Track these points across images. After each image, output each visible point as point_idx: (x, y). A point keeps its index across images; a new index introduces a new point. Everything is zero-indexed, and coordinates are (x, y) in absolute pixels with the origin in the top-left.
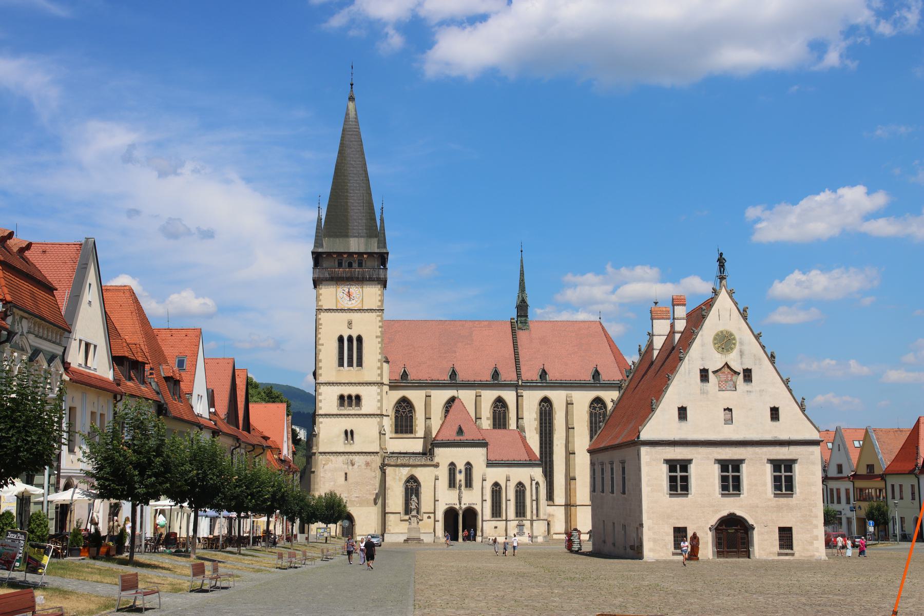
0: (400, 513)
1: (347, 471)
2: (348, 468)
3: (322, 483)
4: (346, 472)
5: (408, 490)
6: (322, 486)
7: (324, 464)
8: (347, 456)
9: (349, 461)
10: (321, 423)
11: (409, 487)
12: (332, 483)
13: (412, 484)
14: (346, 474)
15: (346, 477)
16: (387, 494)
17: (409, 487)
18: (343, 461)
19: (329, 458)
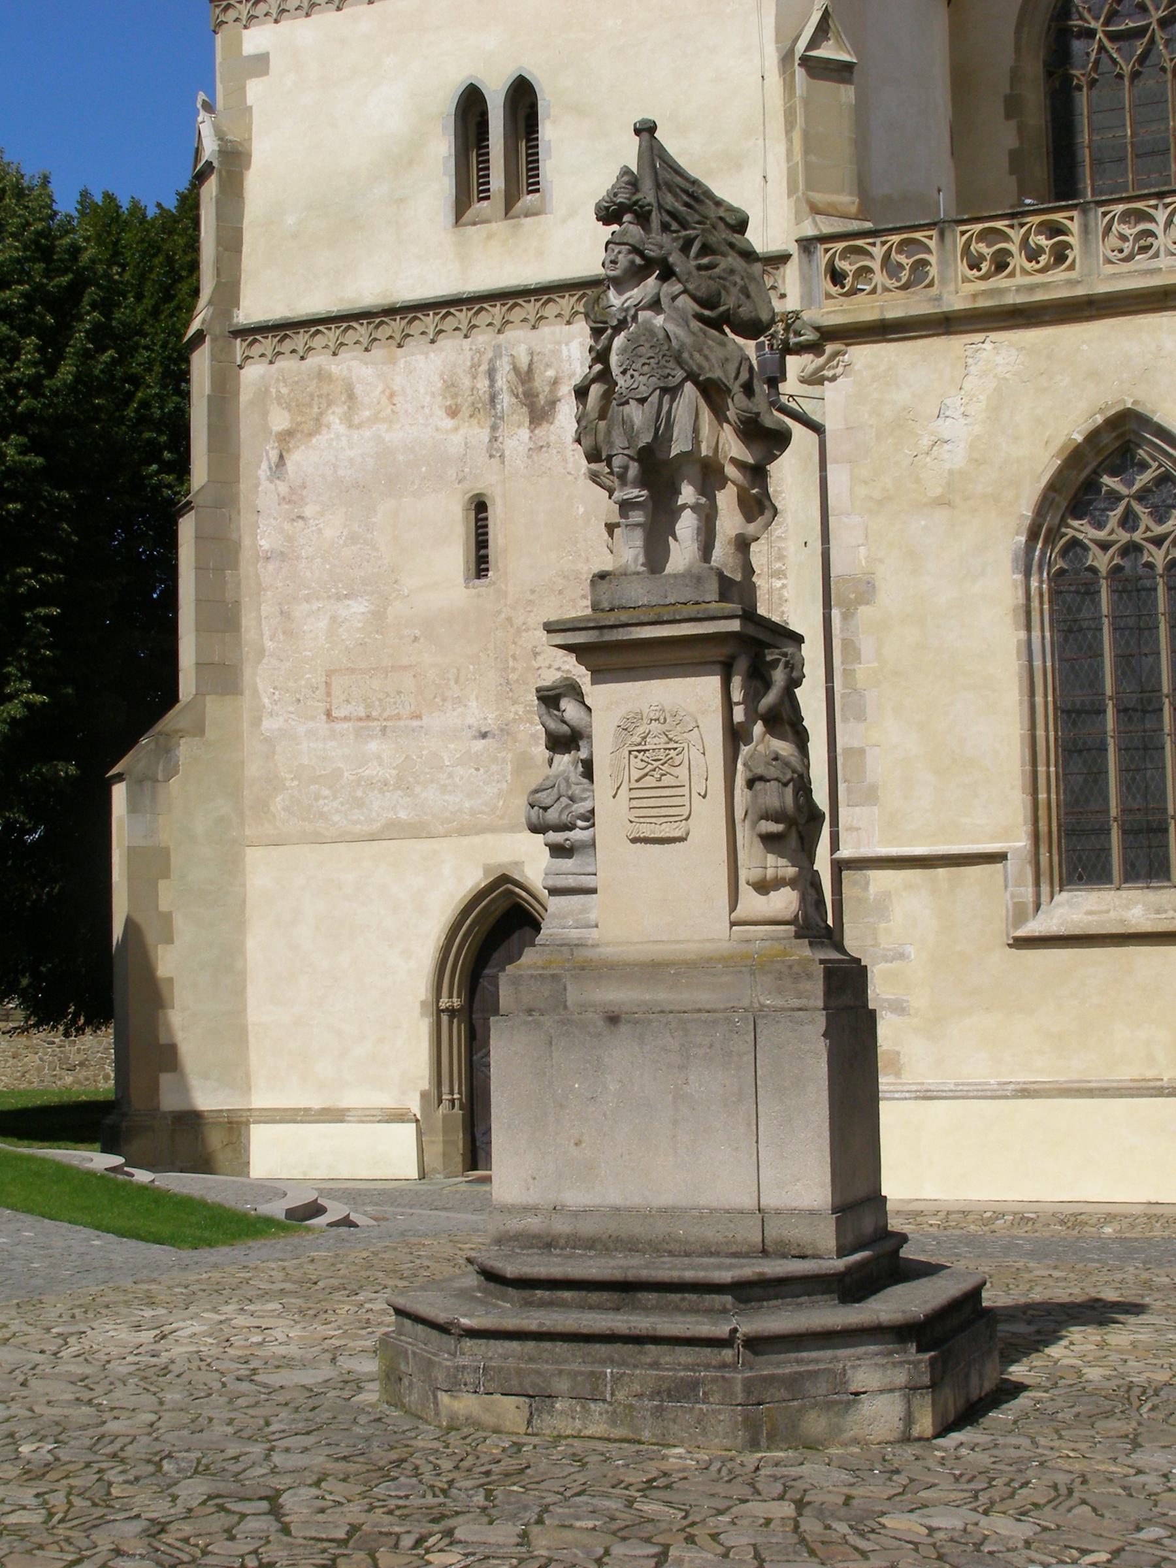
0: (998, 858)
1: (489, 482)
2: (495, 450)
3: (265, 609)
4: (479, 488)
5: (1091, 593)
6: (269, 645)
7: (286, 437)
8: (482, 338)
9: (501, 383)
10: (260, 64)
11: (1102, 561)
12: (358, 608)
13: (1129, 521)
14: (480, 507)
15: (481, 541)
16: (850, 647)
17: (1102, 561)
18: (451, 387)
19: (322, 376)
